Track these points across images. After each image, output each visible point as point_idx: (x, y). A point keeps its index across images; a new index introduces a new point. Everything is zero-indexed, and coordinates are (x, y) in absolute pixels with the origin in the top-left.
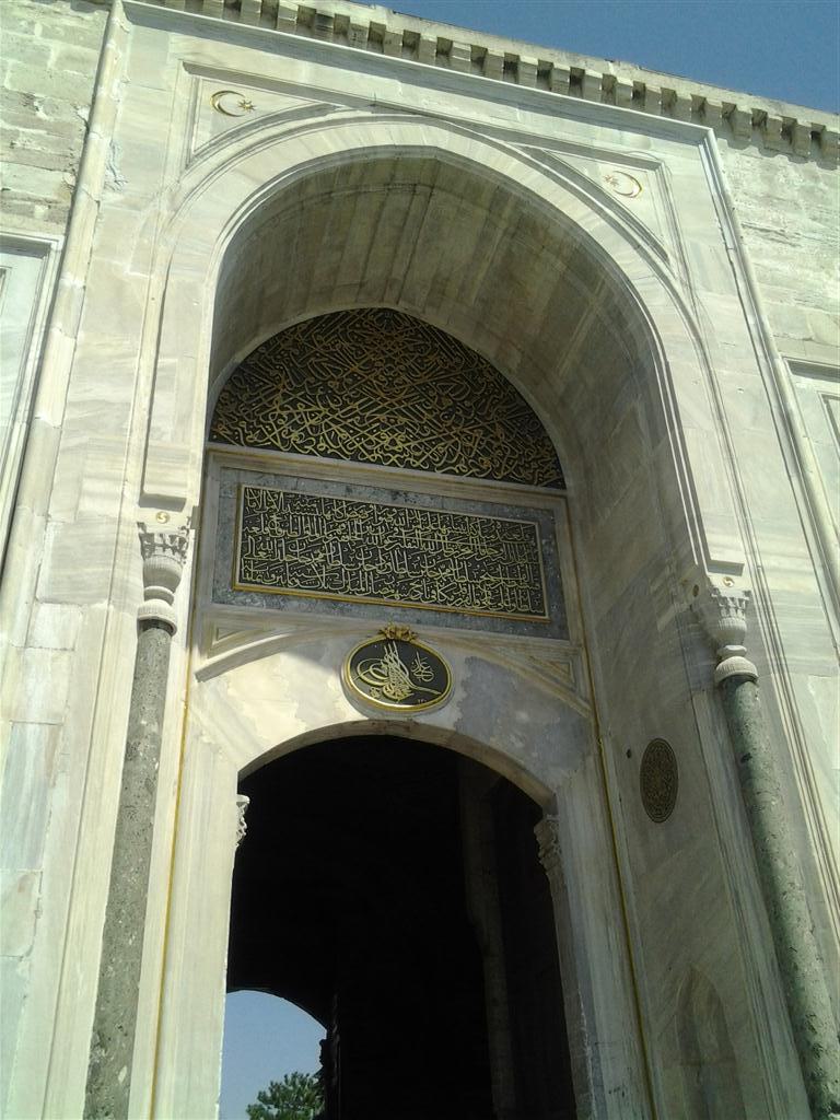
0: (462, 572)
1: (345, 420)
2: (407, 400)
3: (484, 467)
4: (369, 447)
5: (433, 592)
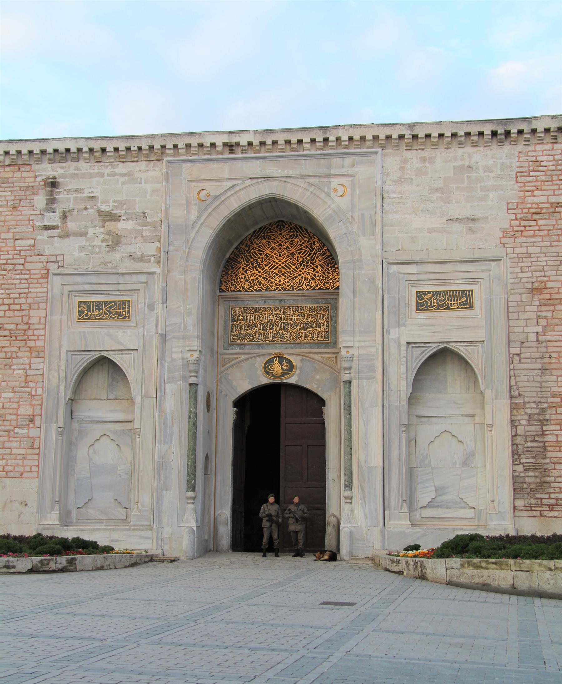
0: (301, 328)
2: (285, 262)
4: (271, 285)
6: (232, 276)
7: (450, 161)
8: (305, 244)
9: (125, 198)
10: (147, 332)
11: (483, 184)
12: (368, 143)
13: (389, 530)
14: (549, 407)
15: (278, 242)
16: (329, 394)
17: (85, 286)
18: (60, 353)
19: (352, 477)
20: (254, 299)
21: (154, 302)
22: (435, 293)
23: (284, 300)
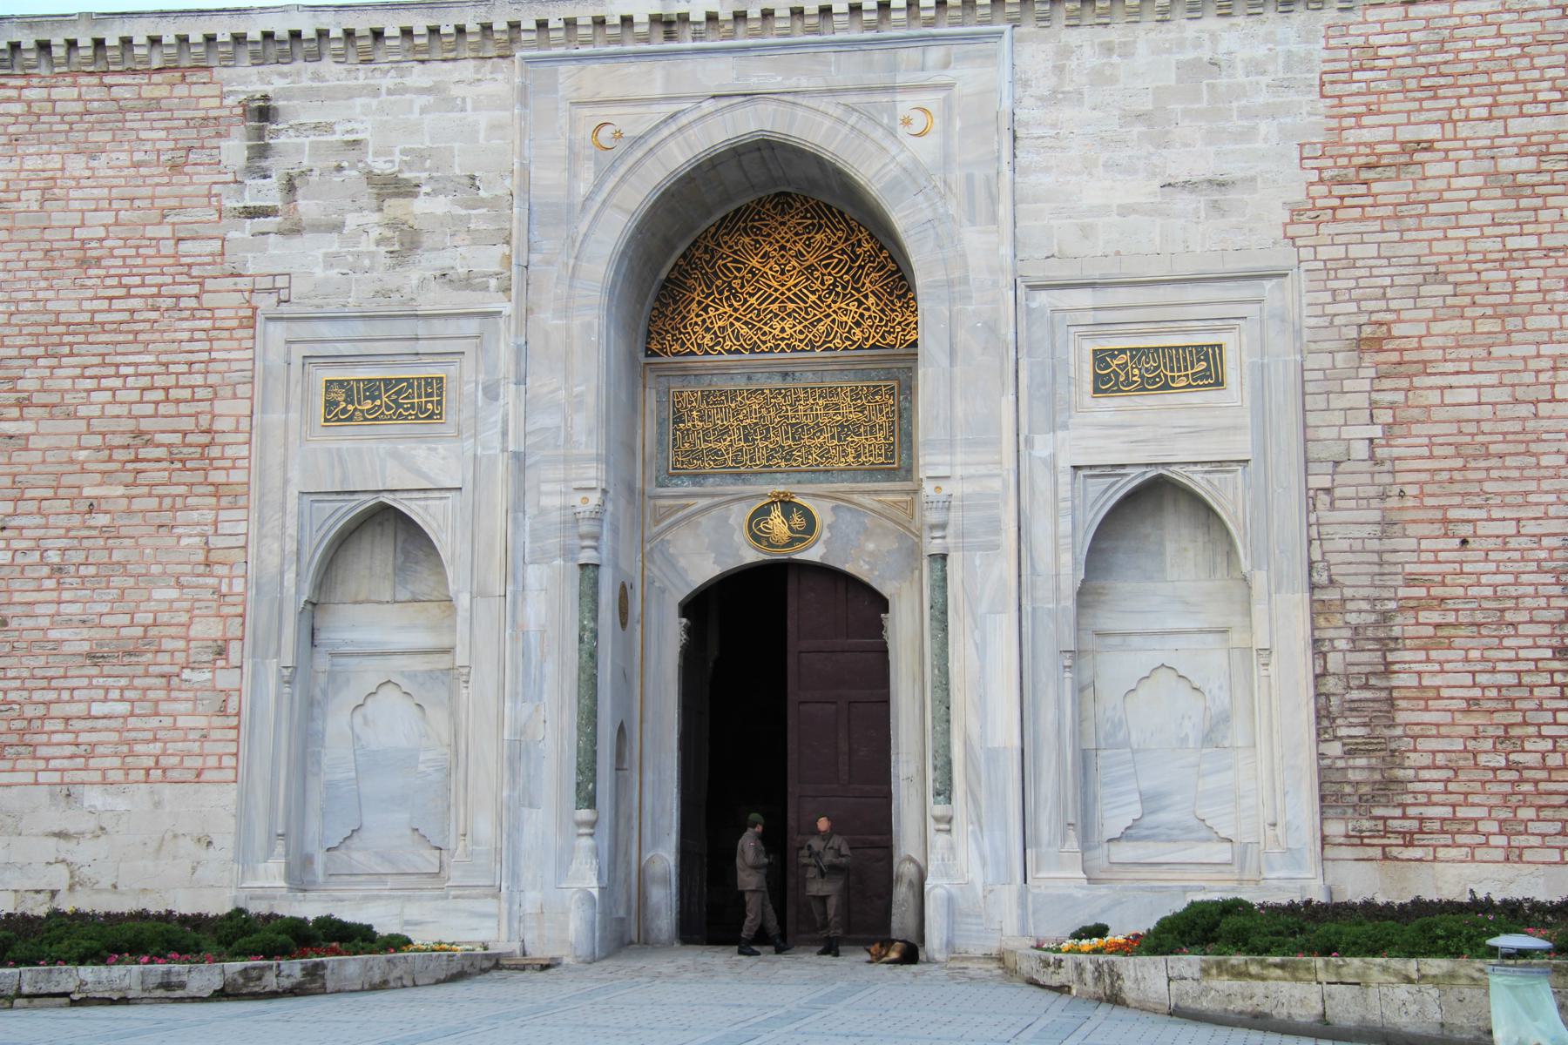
0: (833, 437)
7: (1169, 51)
8: (840, 246)
9: (428, 143)
10: (483, 449)
11: (1244, 102)
12: (980, 11)
13: (1037, 891)
14: (1401, 609)
16: (896, 584)
17: (338, 345)
18: (284, 496)
19: (950, 772)
20: (724, 371)
21: (498, 381)
22: (1137, 353)
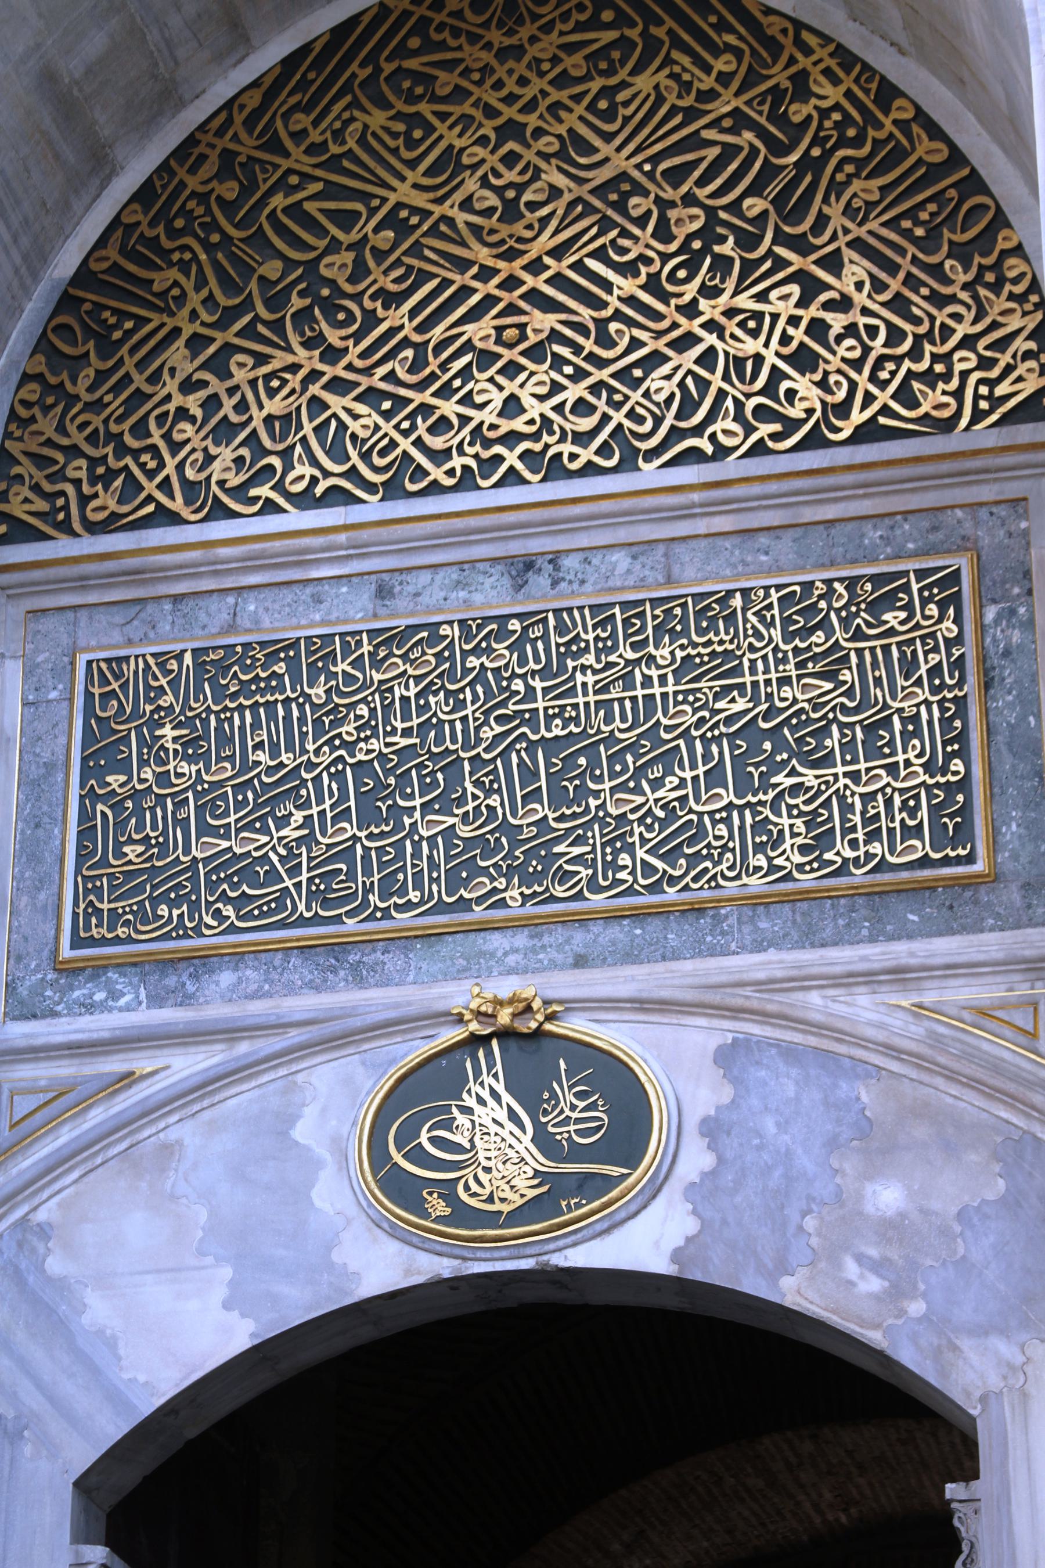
1: (368, 371)
2: (557, 253)
3: (796, 412)
4: (437, 443)
5: (624, 859)
6: (97, 406)
8: (723, 107)
15: (491, 112)
23: (555, 558)
